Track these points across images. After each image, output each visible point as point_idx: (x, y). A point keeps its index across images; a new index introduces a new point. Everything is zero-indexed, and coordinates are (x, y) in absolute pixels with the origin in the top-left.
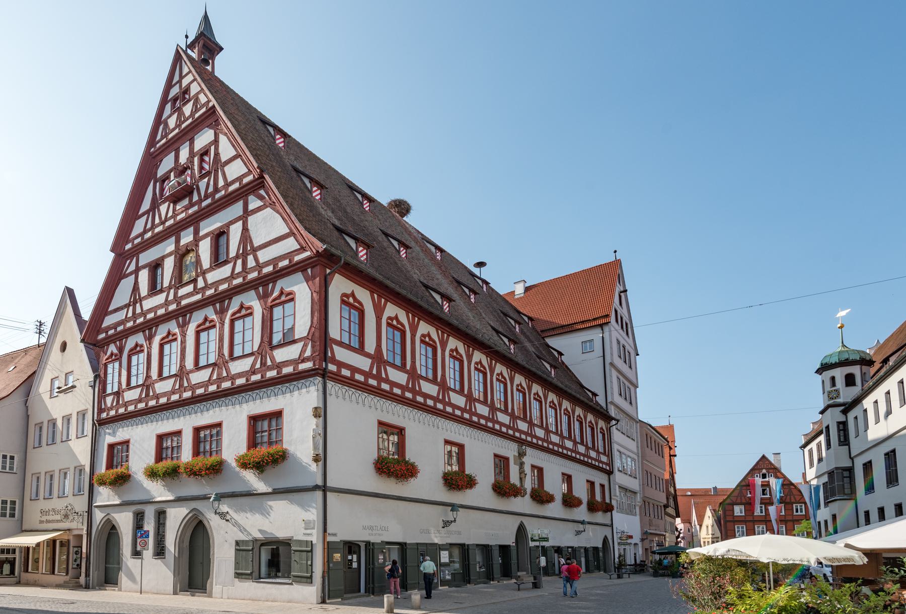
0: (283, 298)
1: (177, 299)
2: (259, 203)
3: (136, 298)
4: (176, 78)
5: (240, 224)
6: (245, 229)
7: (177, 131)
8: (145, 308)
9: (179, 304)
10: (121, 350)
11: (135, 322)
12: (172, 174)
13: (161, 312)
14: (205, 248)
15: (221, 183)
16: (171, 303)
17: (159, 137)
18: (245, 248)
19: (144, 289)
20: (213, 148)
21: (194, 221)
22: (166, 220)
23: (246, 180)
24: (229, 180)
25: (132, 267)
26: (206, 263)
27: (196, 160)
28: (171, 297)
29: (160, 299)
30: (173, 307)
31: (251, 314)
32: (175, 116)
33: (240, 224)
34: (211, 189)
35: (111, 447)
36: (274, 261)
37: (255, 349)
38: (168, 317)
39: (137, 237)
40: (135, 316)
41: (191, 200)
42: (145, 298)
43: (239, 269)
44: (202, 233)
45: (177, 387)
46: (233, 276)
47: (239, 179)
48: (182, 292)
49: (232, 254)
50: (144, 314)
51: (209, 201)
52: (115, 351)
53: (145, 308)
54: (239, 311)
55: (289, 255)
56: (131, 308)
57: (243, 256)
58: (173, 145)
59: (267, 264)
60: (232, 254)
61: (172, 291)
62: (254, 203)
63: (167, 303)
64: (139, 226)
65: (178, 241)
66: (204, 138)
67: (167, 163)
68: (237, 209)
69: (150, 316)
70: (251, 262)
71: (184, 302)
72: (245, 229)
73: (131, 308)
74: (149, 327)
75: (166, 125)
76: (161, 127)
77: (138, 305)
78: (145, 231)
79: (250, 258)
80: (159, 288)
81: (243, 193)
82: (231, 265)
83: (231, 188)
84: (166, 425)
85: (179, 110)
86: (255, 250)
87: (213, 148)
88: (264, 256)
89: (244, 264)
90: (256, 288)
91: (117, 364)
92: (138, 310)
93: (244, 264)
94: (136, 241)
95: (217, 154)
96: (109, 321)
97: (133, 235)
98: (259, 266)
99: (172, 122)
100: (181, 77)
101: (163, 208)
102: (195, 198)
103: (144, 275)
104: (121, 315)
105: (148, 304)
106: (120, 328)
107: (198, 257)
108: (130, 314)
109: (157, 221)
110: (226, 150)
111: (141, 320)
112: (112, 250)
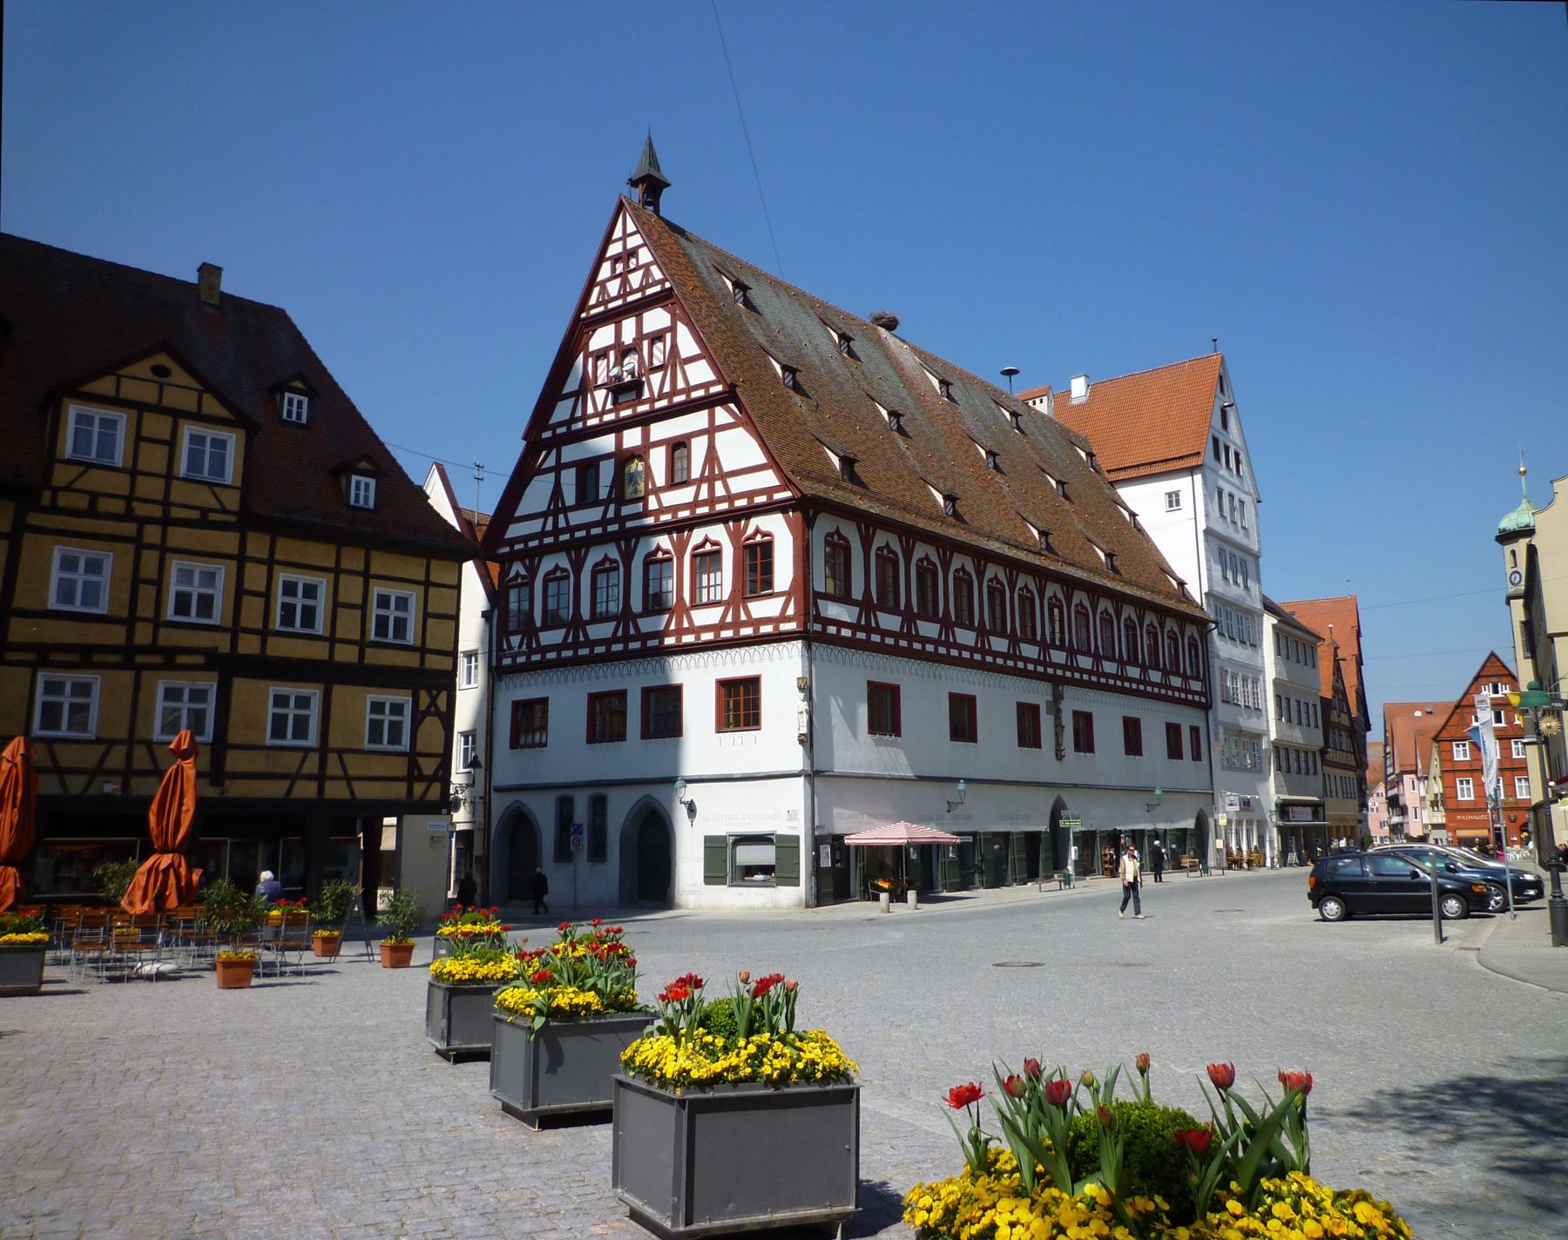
0: (758, 538)
1: (619, 519)
2: (731, 420)
3: (556, 505)
4: (618, 233)
5: (705, 438)
6: (711, 448)
7: (619, 302)
8: (572, 523)
9: (622, 525)
10: (533, 571)
11: (556, 538)
12: (612, 354)
13: (596, 531)
14: (658, 458)
15: (681, 385)
16: (612, 521)
17: (593, 301)
18: (712, 470)
19: (570, 498)
20: (668, 336)
21: (644, 421)
22: (604, 412)
23: (713, 390)
24: (692, 383)
25: (551, 462)
26: (660, 480)
27: (646, 343)
28: (611, 514)
29: (594, 514)
30: (613, 528)
31: (719, 552)
32: (618, 281)
33: (705, 438)
34: (667, 389)
35: (519, 706)
36: (750, 495)
37: (725, 597)
38: (604, 539)
39: (560, 424)
40: (556, 531)
41: (640, 394)
42: (572, 509)
43: (704, 495)
44: (652, 439)
45: (620, 633)
46: (696, 503)
47: (706, 385)
48: (626, 510)
49: (696, 473)
50: (570, 529)
51: (664, 403)
52: (523, 572)
53: (572, 523)
54: (702, 545)
55: (769, 491)
56: (550, 519)
57: (710, 479)
58: (614, 317)
59: (740, 496)
60: (696, 473)
61: (612, 507)
62: (722, 416)
63: (604, 522)
64: (562, 411)
65: (619, 442)
66: (656, 319)
67: (602, 337)
68: (699, 420)
69: (580, 534)
70: (720, 491)
71: (629, 524)
72: (711, 448)
73: (550, 519)
74: (577, 548)
75: (604, 290)
76: (596, 290)
77: (561, 517)
78: (573, 420)
79: (719, 485)
80: (591, 499)
81: (708, 403)
82: (693, 488)
83: (694, 395)
84: (606, 680)
85: (624, 277)
86: (724, 476)
87: (668, 336)
88: (738, 485)
89: (711, 490)
90: (725, 521)
91: (525, 591)
92: (562, 524)
93: (711, 490)
94: (560, 430)
95: (674, 346)
96: (514, 531)
97: (555, 419)
98: (730, 498)
99: (613, 288)
100: (625, 236)
101: (600, 395)
102: (646, 394)
103: (569, 477)
104: (535, 526)
105: (576, 518)
106: (532, 544)
107: (648, 469)
108: (549, 527)
109: (590, 410)
110: (687, 344)
111: (564, 537)
112: (525, 438)
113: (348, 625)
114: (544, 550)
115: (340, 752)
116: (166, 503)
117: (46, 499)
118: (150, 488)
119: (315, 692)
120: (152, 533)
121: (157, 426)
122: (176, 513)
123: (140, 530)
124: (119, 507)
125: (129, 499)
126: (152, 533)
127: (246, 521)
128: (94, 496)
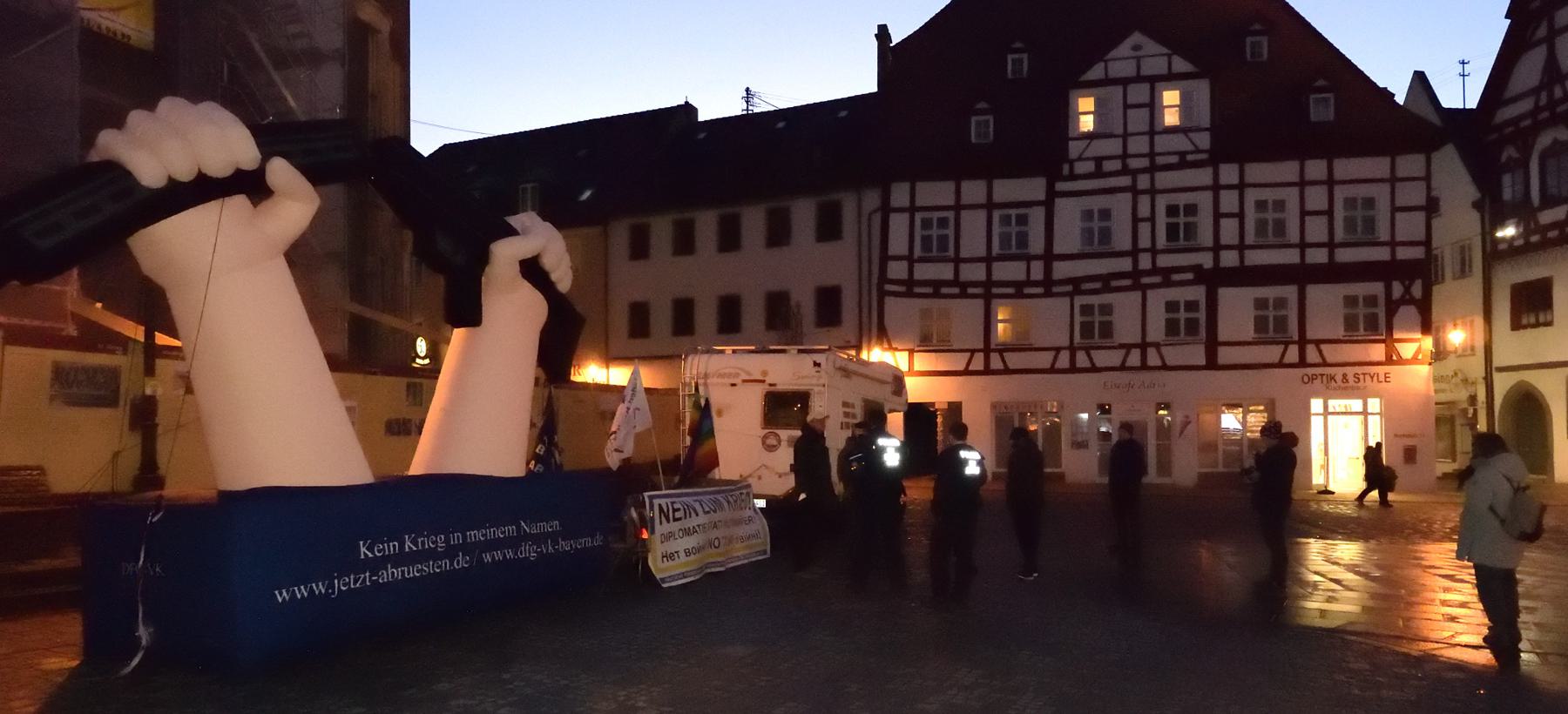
113: (1317, 230)
114: (1538, 128)
115: (1318, 343)
116: (1152, 155)
117: (1066, 169)
118: (1138, 145)
119: (1290, 292)
120: (1143, 182)
121: (1139, 93)
122: (1160, 160)
123: (1134, 181)
124: (1115, 165)
125: (1125, 156)
126: (1143, 182)
127: (1215, 158)
128: (1099, 161)
